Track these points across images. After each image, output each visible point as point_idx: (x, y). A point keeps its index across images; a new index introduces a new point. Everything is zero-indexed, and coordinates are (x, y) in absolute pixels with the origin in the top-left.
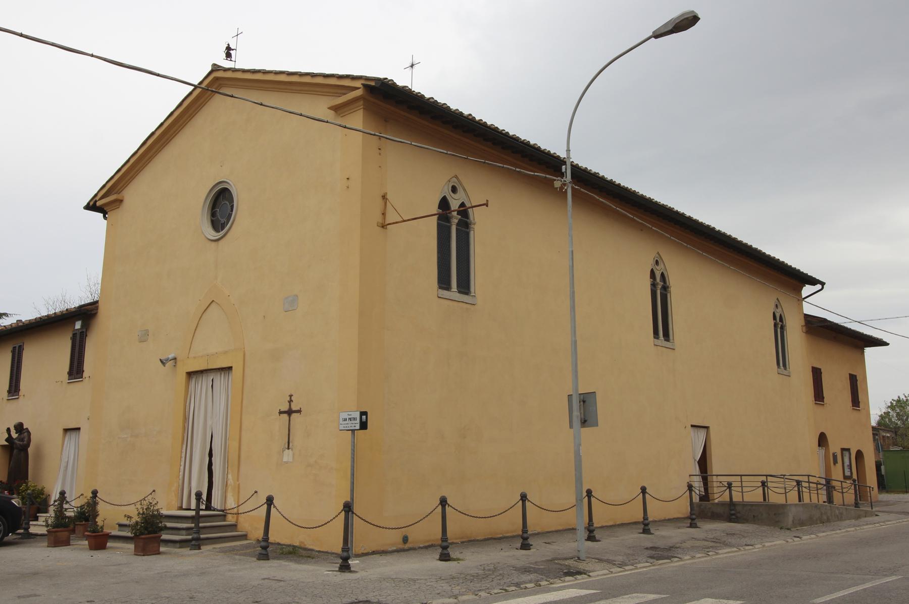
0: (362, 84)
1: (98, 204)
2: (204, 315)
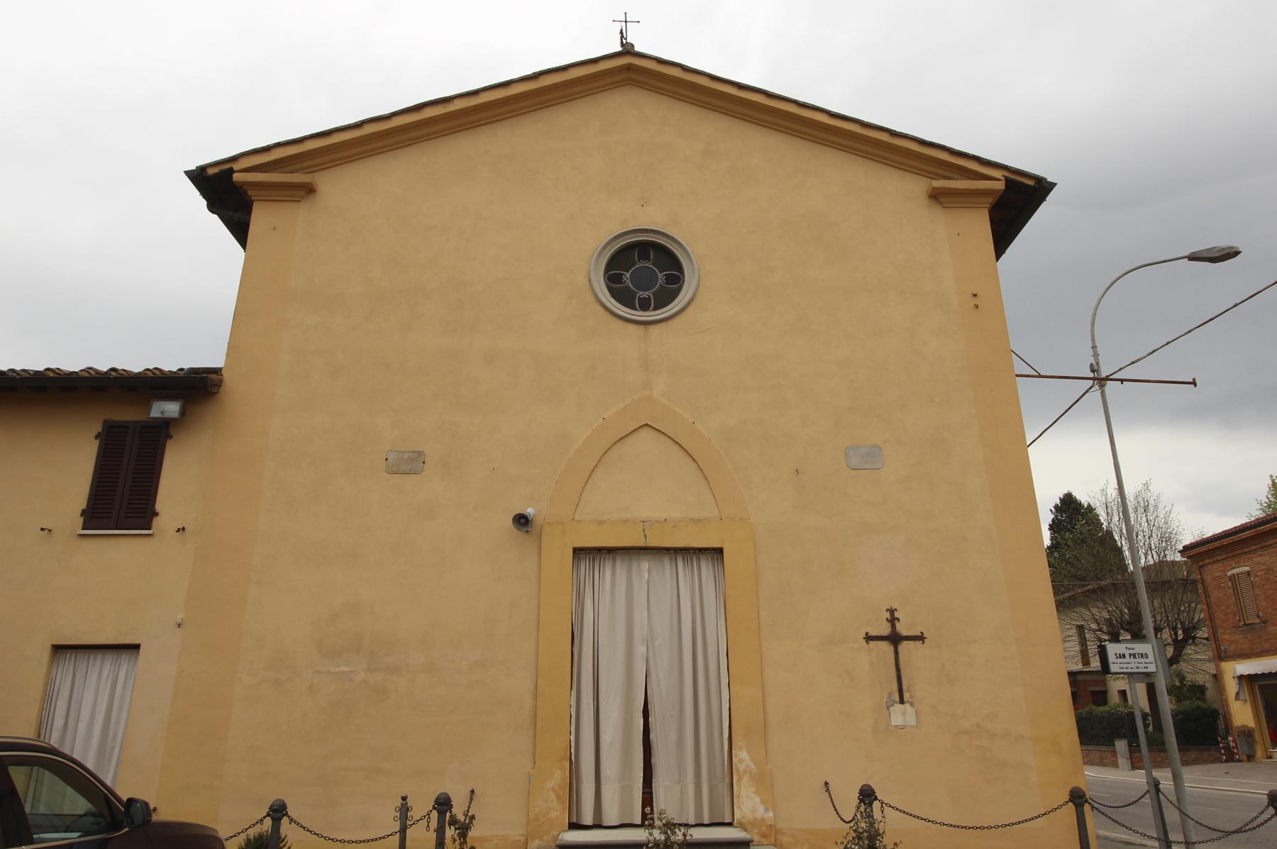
0: (1003, 176)
2: (614, 447)
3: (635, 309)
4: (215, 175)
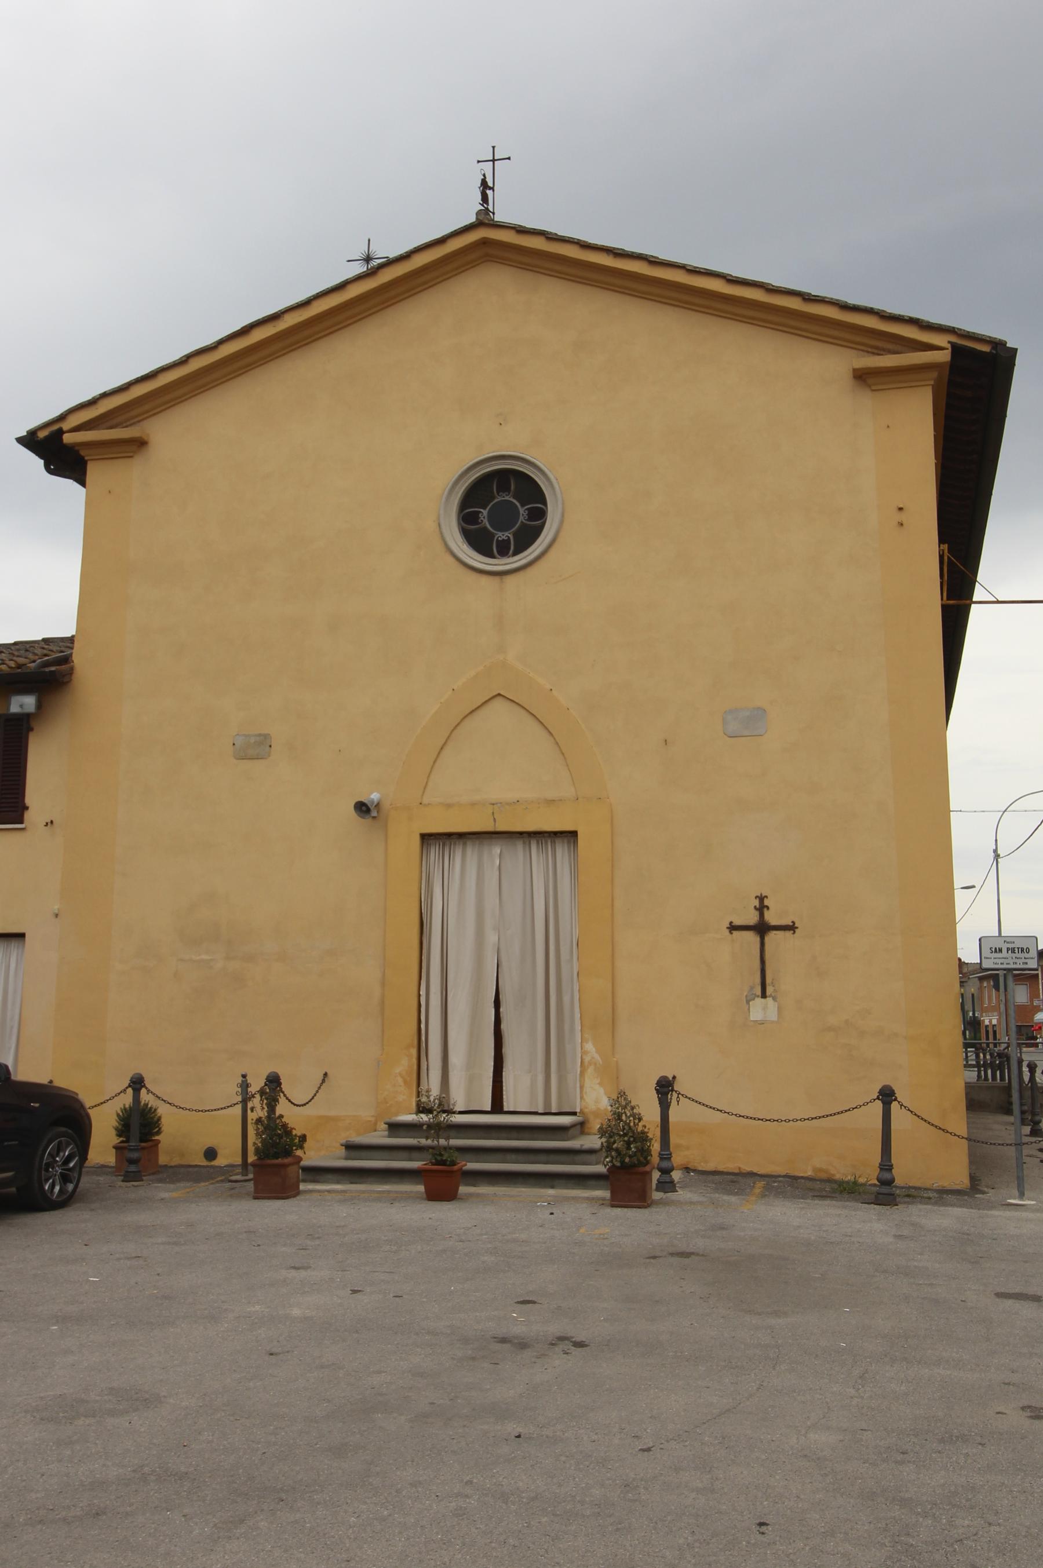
0: (949, 342)
1: (68, 438)
3: (492, 556)
4: (46, 438)
